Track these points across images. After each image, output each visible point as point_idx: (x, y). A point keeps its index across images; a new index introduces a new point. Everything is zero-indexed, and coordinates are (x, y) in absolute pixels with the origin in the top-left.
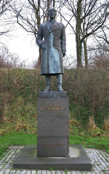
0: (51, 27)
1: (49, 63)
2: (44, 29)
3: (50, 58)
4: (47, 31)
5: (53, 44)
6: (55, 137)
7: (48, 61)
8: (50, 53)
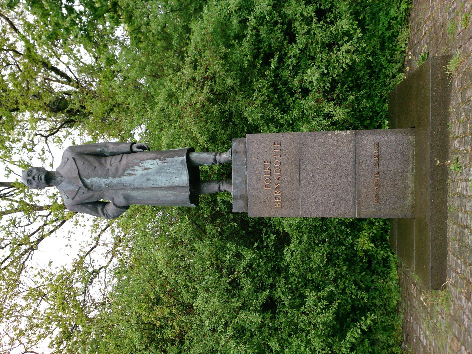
0: (69, 183)
1: (163, 185)
2: (77, 199)
3: (149, 184)
4: (81, 191)
5: (114, 176)
6: (355, 168)
7: (159, 188)
8: (136, 185)
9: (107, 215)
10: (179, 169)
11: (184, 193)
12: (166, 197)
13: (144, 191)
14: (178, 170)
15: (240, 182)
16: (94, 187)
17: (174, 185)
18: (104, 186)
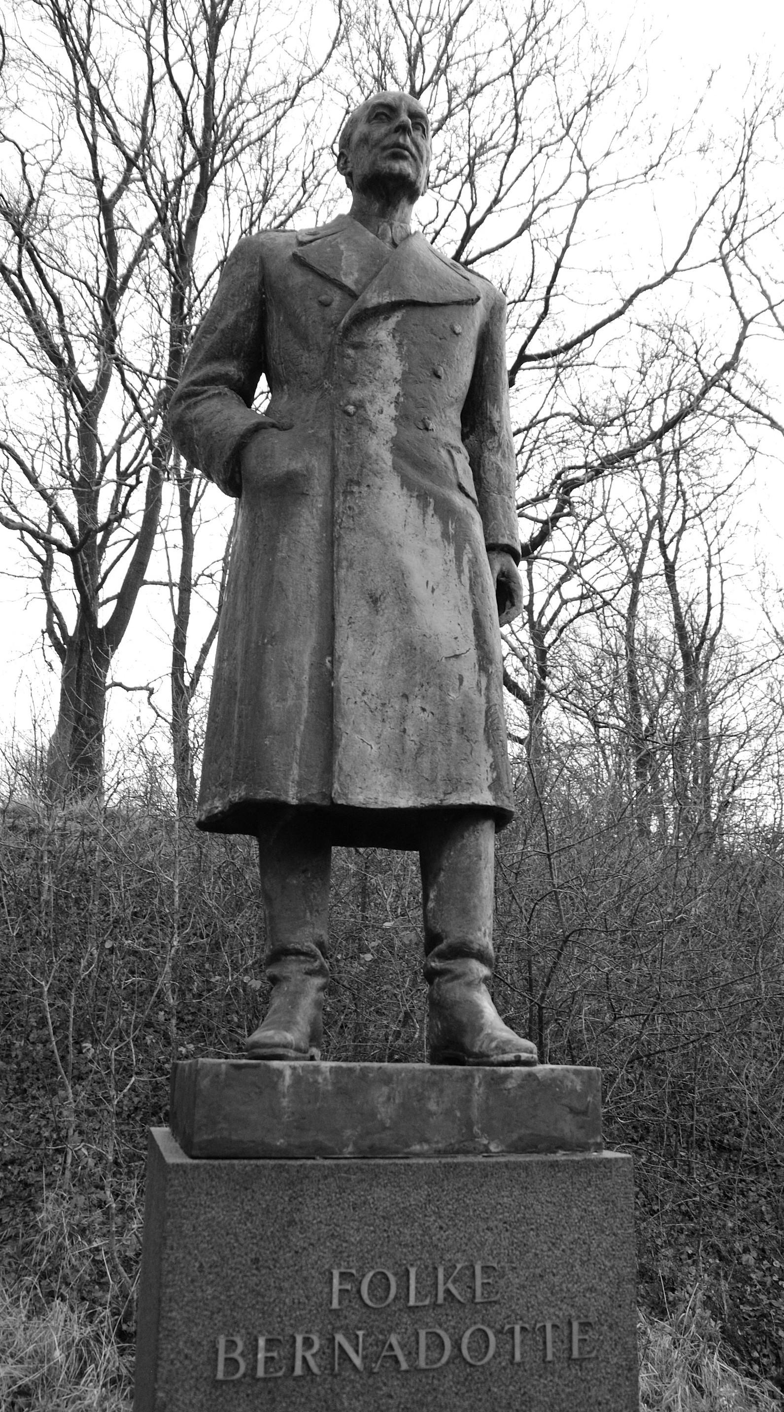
1: (343, 669)
3: (351, 605)
4: (337, 297)
5: (398, 448)
7: (328, 646)
8: (351, 541)
9: (197, 394)
10: (425, 762)
11: (295, 772)
12: (283, 676)
13: (316, 570)
14: (419, 753)
15: (373, 1115)
16: (351, 352)
17: (343, 726)
18: (355, 394)
